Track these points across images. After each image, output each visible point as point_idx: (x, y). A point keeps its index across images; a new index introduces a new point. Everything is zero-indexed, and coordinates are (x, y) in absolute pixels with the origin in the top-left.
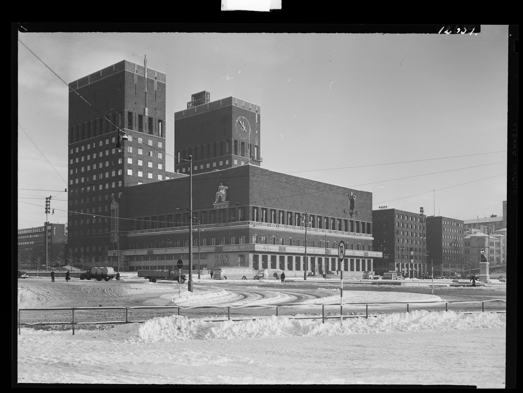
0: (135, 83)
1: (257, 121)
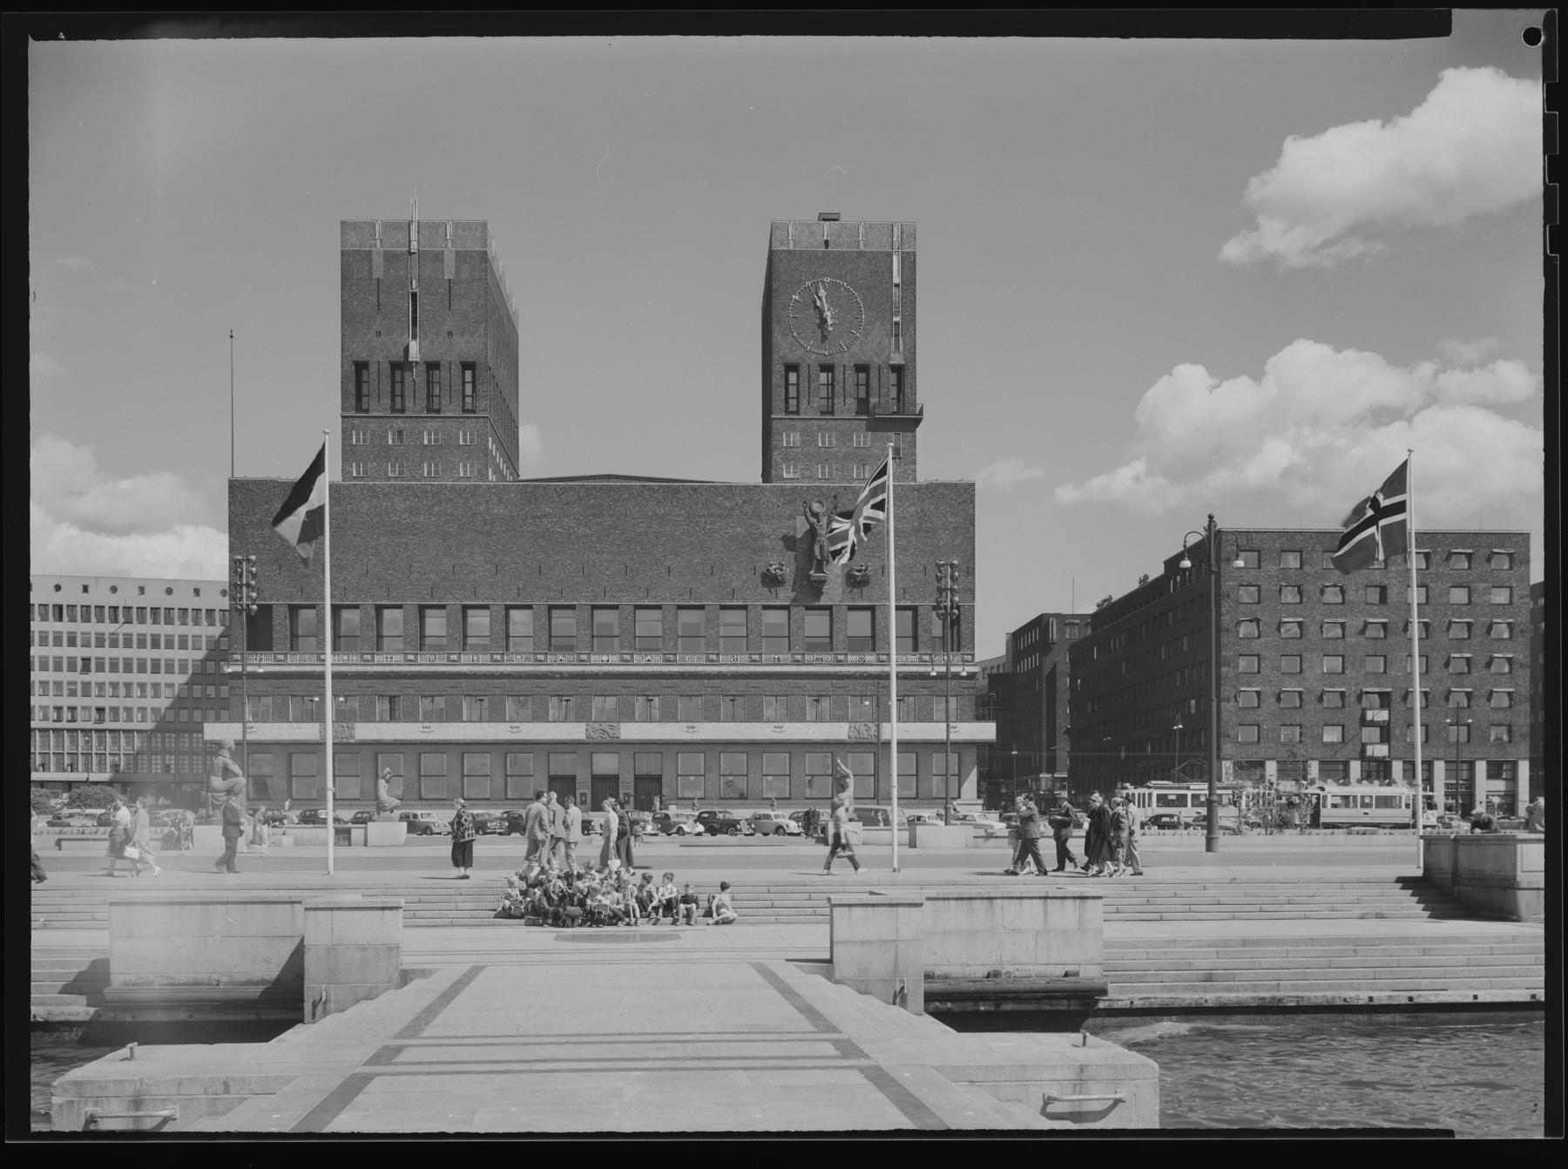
0: (378, 273)
1: (897, 279)
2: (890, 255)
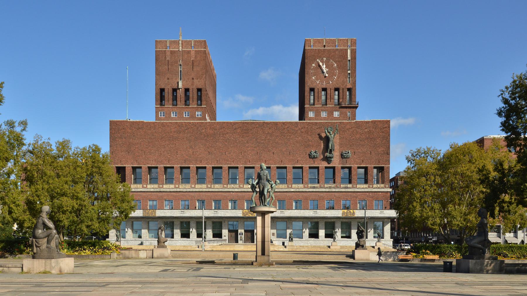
1: (349, 58)
2: (347, 50)
